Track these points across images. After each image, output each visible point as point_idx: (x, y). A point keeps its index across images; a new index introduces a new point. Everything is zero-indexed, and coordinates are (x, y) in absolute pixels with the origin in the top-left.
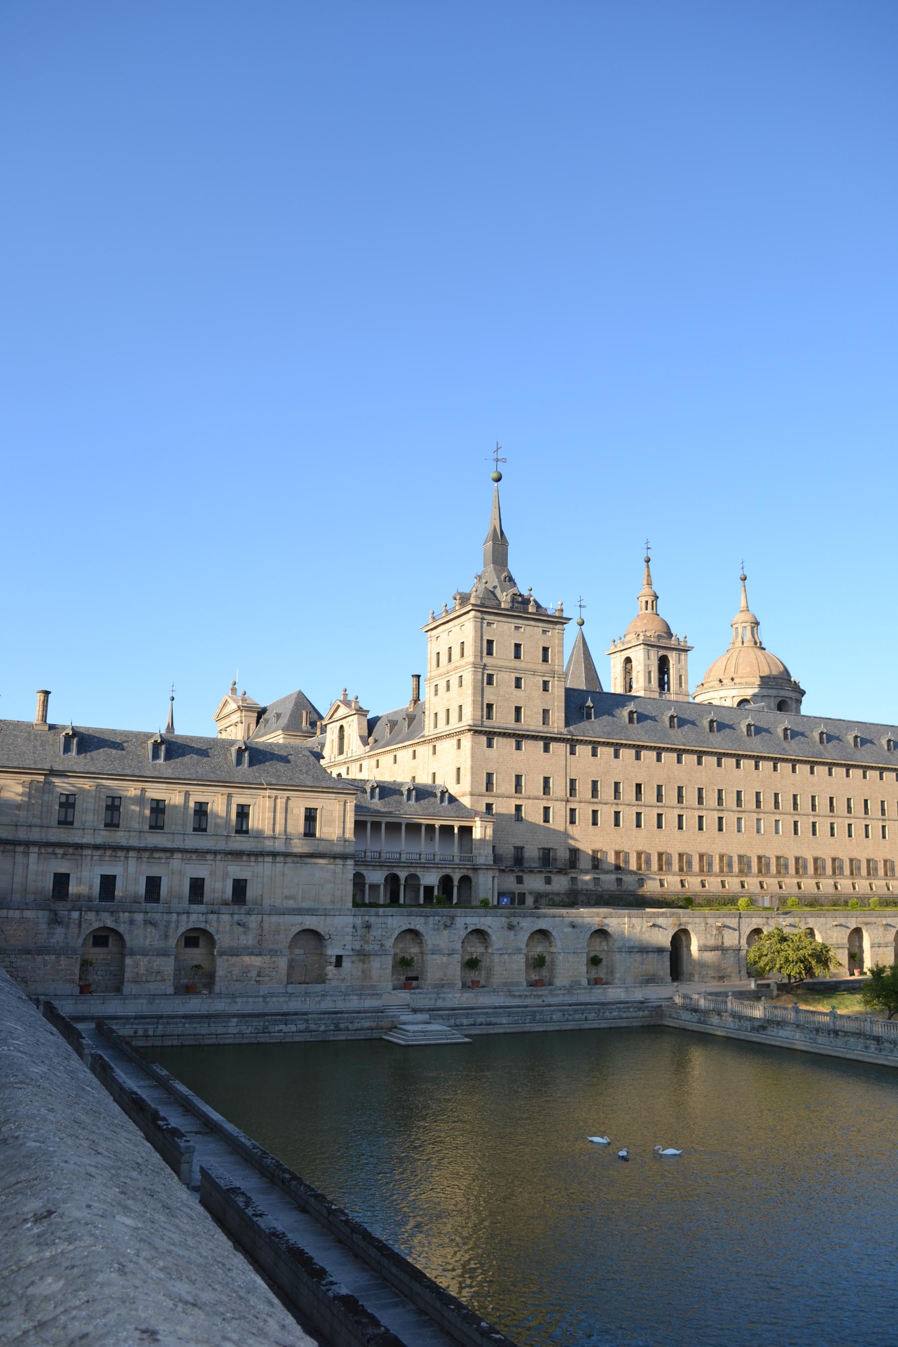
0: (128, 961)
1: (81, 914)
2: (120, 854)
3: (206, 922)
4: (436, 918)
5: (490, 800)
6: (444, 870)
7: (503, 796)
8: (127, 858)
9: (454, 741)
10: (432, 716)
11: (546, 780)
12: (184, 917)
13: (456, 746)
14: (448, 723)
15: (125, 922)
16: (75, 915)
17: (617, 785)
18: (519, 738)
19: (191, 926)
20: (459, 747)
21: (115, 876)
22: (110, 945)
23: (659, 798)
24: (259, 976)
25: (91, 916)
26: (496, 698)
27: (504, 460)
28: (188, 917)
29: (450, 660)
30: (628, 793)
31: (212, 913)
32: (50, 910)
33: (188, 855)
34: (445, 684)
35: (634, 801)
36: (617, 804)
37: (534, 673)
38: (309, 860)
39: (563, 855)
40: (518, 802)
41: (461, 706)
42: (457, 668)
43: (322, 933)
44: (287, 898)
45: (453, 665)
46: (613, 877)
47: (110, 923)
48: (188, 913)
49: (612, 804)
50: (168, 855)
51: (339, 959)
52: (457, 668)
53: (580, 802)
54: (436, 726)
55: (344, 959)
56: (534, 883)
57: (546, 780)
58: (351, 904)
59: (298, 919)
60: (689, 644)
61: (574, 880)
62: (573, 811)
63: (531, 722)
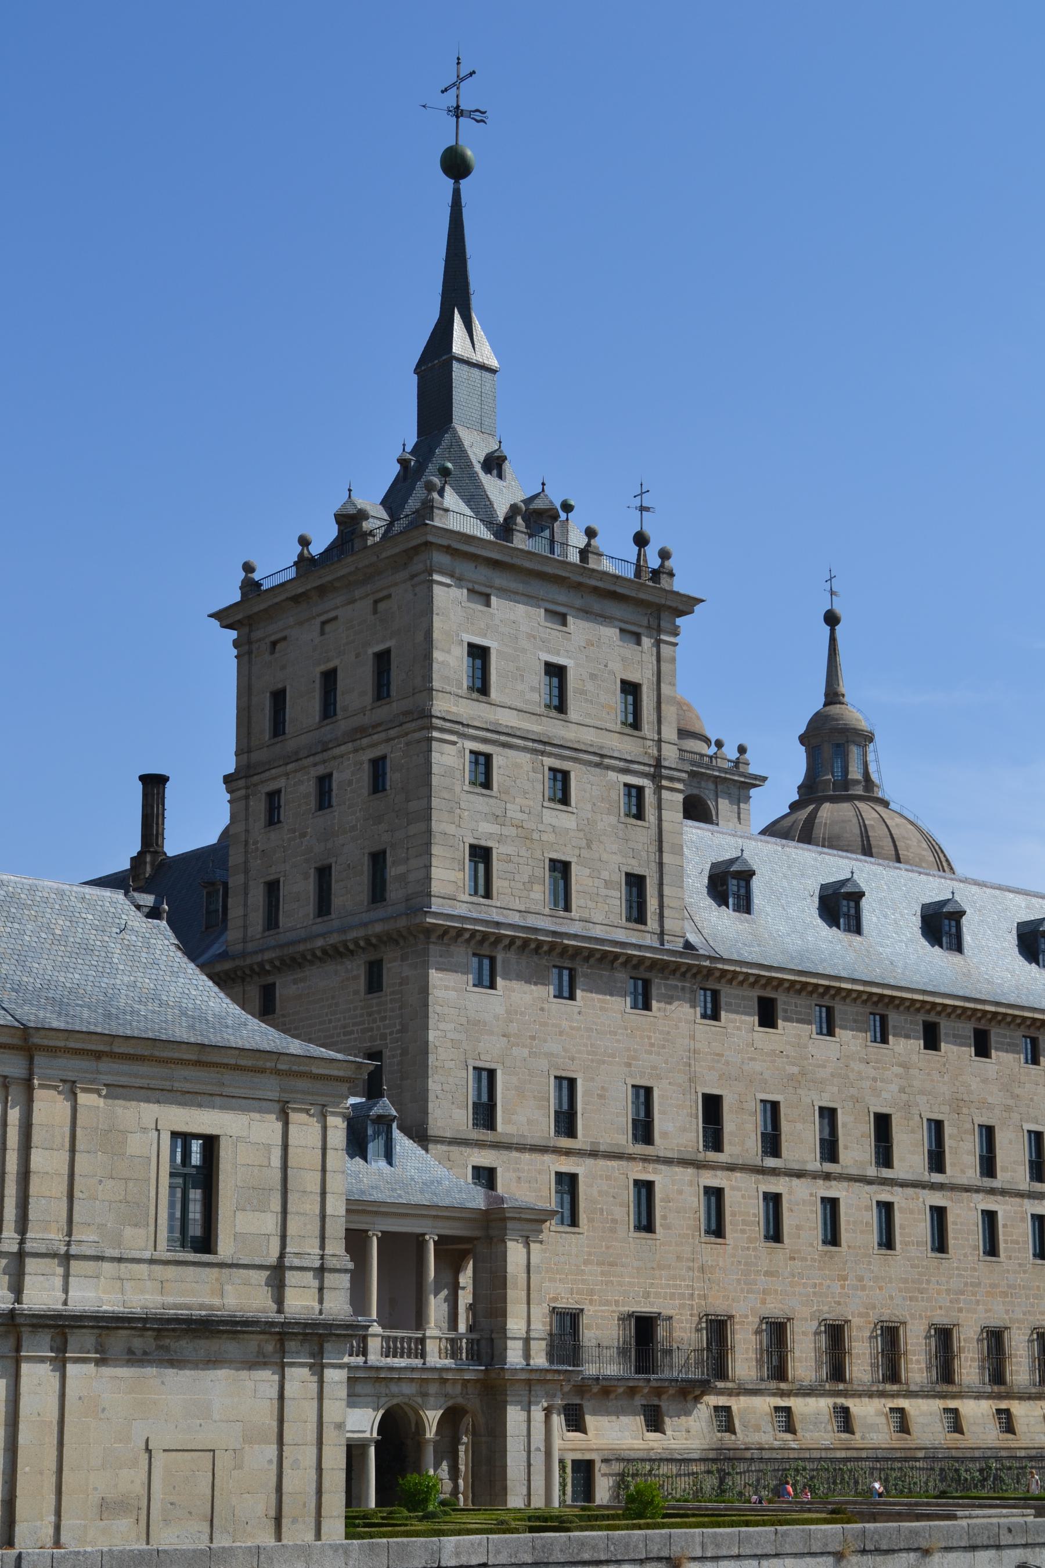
5: (485, 1158)
6: (394, 1388)
7: (522, 1148)
9: (356, 969)
10: (257, 895)
11: (644, 1096)
13: (362, 984)
14: (324, 905)
17: (829, 1115)
18: (568, 964)
20: (374, 983)
23: (937, 1161)
26: (494, 829)
27: (479, 116)
29: (329, 709)
30: (856, 1149)
34: (309, 787)
35: (872, 1171)
36: (827, 1176)
37: (600, 760)
38: (185, 1346)
39: (683, 1334)
40: (567, 1165)
41: (378, 859)
42: (361, 731)
44: (107, 1508)
45: (343, 724)
46: (824, 1404)
49: (815, 1176)
52: (361, 731)
53: (731, 1168)
54: (272, 921)
56: (615, 1433)
57: (644, 1096)
58: (335, 1527)
60: (752, 770)
61: (725, 1418)
62: (715, 1195)
63: (597, 913)
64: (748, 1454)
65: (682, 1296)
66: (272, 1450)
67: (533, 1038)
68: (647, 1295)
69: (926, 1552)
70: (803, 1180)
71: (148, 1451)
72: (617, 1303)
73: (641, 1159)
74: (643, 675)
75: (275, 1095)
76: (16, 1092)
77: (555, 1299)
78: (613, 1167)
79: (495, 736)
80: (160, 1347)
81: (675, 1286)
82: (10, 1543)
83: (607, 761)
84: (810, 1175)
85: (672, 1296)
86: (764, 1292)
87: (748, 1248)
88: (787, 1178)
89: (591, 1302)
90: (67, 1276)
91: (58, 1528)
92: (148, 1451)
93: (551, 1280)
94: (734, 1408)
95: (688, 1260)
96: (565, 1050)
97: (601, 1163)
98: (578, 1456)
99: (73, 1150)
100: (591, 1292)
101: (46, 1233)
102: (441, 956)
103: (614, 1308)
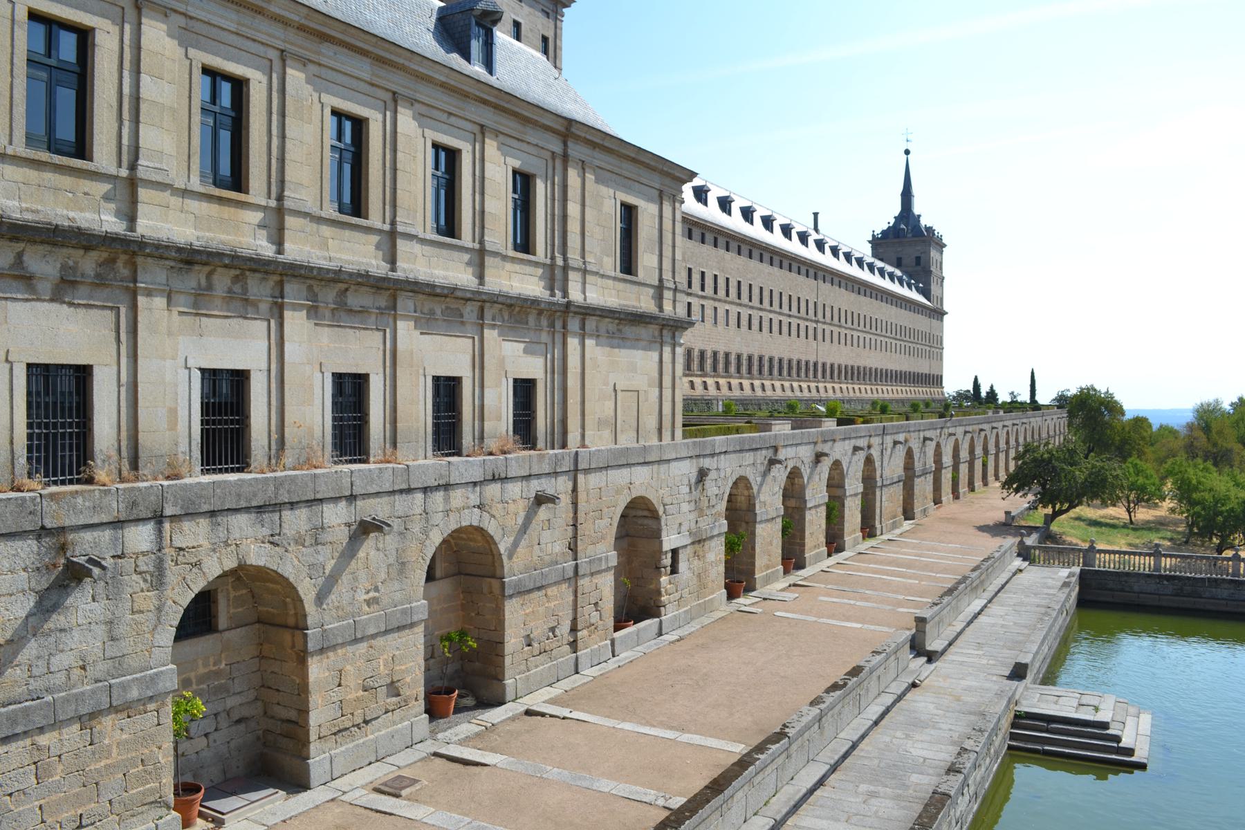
0: (317, 670)
1: (160, 532)
2: (259, 289)
3: (480, 507)
4: (764, 452)
8: (278, 311)
12: (439, 496)
15: (300, 541)
16: (140, 537)
19: (454, 526)
21: (240, 378)
22: (223, 622)
24: (574, 629)
25: (194, 534)
28: (447, 500)
31: (494, 479)
32: (43, 532)
33: (428, 304)
38: (629, 331)
43: (655, 502)
44: (601, 423)
47: (258, 556)
48: (447, 487)
50: (382, 301)
51: (675, 552)
55: (682, 556)
59: (619, 477)
66: (657, 390)
69: (834, 441)
71: (615, 390)
74: (550, 34)
75: (657, 186)
76: (558, 163)
80: (619, 330)
82: (564, 445)
90: (584, 283)
91: (583, 436)
92: (615, 390)
99: (583, 205)
101: (574, 255)
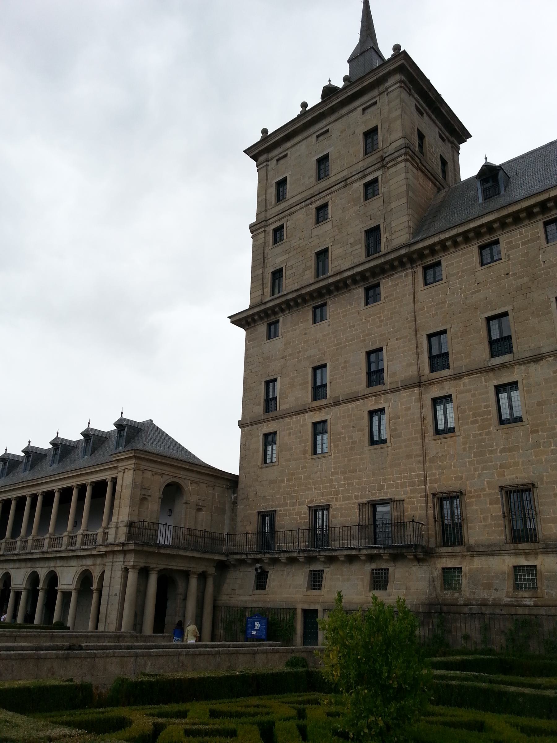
64: (466, 610)
65: (412, 484)
67: (300, 352)
68: (381, 488)
70: (542, 363)
72: (356, 497)
73: (373, 396)
77: (312, 501)
78: (353, 408)
79: (283, 214)
81: (405, 477)
83: (349, 181)
84: (550, 356)
85: (403, 485)
86: (502, 466)
87: (481, 434)
88: (523, 367)
89: (337, 501)
93: (309, 489)
94: (466, 568)
95: (417, 455)
96: (319, 350)
97: (343, 407)
98: (306, 607)
100: (337, 493)
102: (251, 334)
103: (355, 501)
